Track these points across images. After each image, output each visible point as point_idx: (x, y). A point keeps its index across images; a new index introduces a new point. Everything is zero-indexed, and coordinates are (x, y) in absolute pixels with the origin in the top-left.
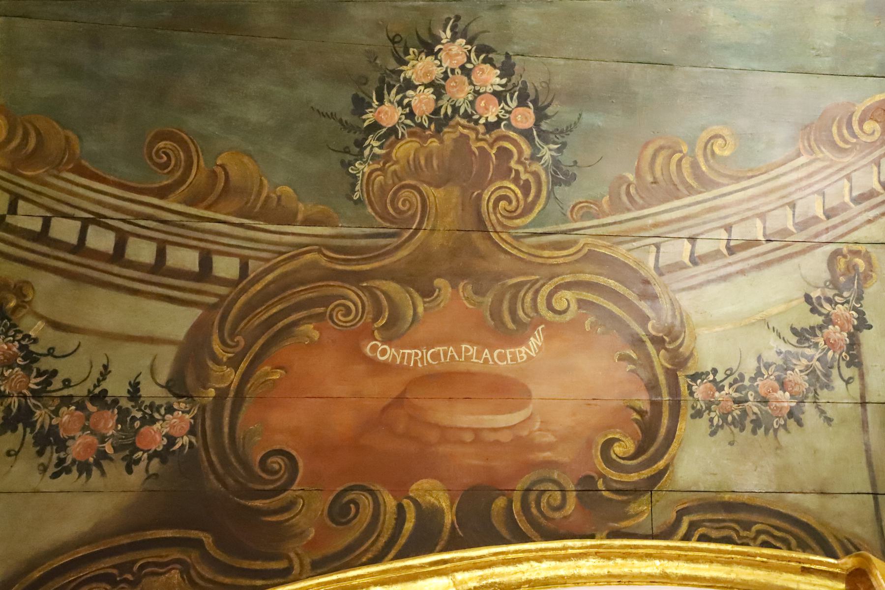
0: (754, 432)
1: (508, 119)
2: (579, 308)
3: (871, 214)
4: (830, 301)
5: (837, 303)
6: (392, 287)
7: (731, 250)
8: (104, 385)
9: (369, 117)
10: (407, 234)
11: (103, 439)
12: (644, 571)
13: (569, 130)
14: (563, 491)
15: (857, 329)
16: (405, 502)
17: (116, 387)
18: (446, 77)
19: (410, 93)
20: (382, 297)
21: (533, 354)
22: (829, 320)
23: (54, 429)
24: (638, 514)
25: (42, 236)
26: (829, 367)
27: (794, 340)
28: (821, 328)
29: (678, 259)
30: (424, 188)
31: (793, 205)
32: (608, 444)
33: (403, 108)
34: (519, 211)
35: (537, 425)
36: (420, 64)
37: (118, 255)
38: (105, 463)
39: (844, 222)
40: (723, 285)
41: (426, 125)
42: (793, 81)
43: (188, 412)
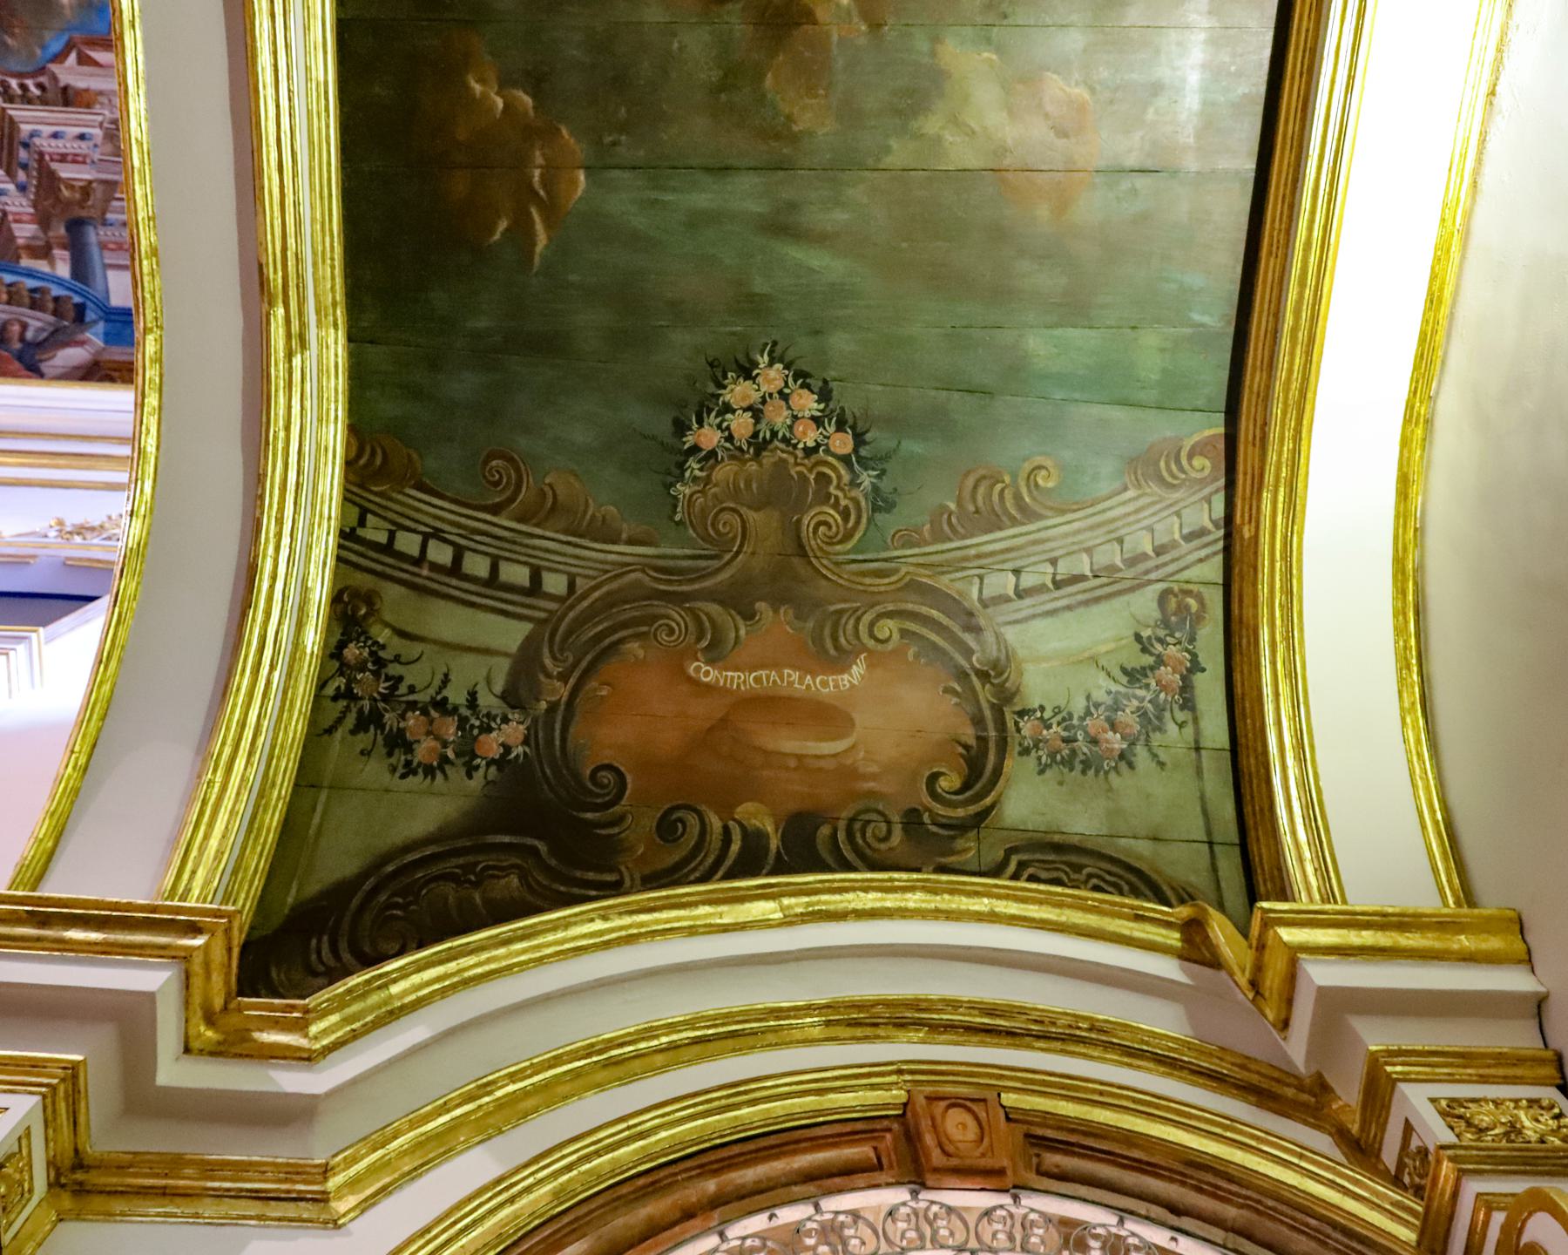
0: (1084, 772)
1: (827, 445)
2: (902, 637)
3: (1203, 553)
4: (1161, 641)
5: (1168, 644)
6: (714, 609)
7: (1058, 585)
9: (690, 440)
10: (727, 557)
13: (887, 457)
15: (1190, 671)
18: (764, 402)
19: (729, 416)
20: (704, 618)
21: (856, 682)
22: (1160, 661)
25: (388, 548)
26: (1160, 710)
27: (1124, 680)
28: (1152, 668)
29: (1002, 592)
30: (743, 510)
31: (1120, 541)
33: (722, 431)
34: (839, 537)
36: (738, 388)
37: (455, 569)
39: (1173, 561)
40: (1049, 621)
41: (745, 448)
42: (1116, 413)
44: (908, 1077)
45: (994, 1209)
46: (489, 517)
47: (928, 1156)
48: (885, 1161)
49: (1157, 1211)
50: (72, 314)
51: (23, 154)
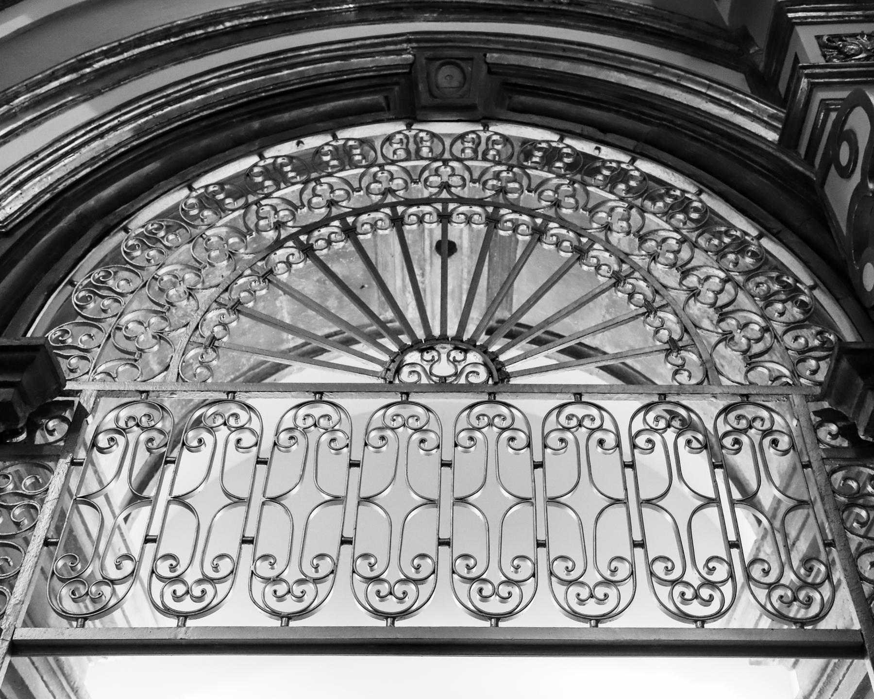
44: (414, 45)
45: (467, 133)
48: (392, 106)
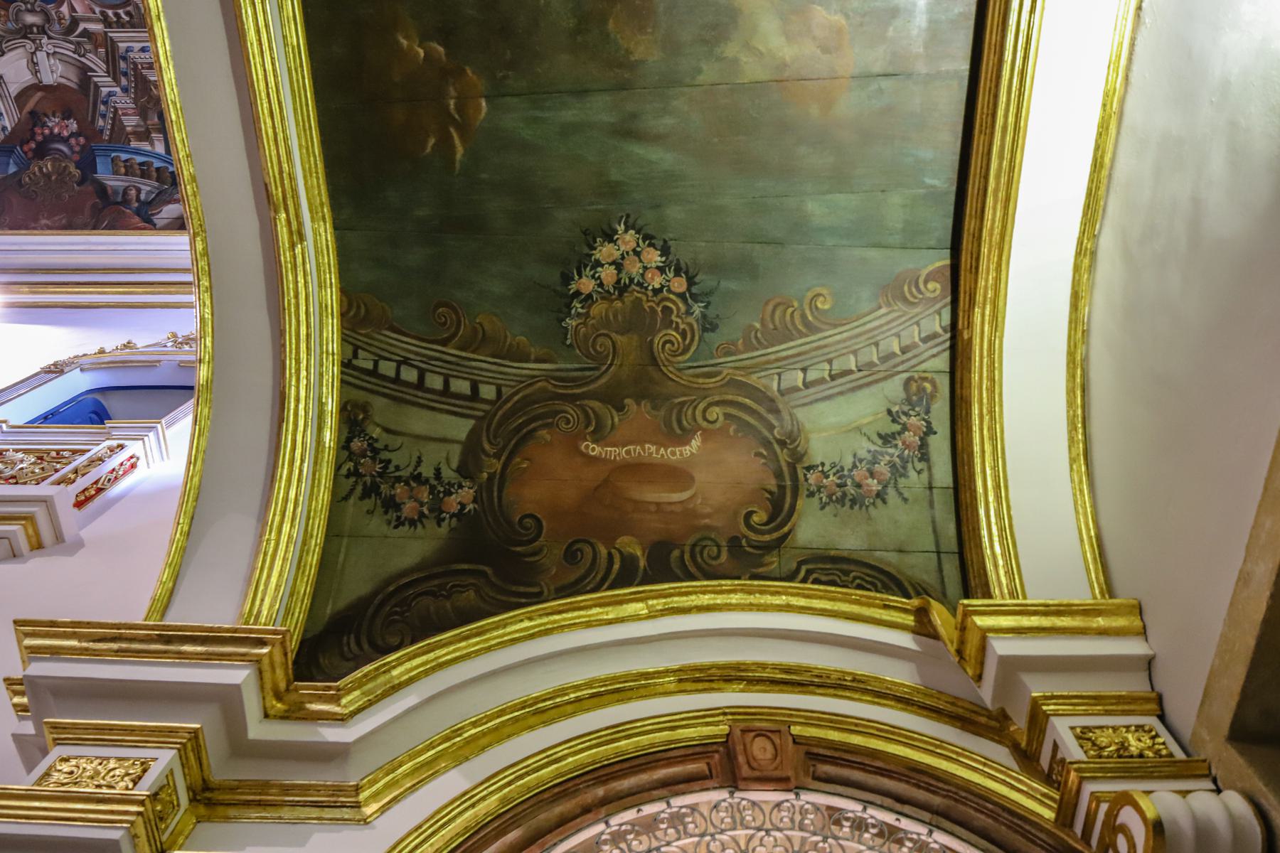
0: (852, 507)
1: (668, 286)
2: (725, 419)
3: (935, 351)
4: (906, 414)
5: (911, 416)
6: (596, 404)
7: (833, 378)
8: (419, 470)
9: (573, 287)
10: (604, 368)
11: (422, 504)
12: (774, 602)
13: (710, 293)
14: (718, 546)
15: (926, 434)
16: (613, 551)
17: (427, 471)
18: (623, 258)
19: (599, 269)
20: (590, 411)
21: (694, 451)
22: (905, 428)
23: (393, 497)
24: (772, 563)
25: (374, 373)
26: (905, 461)
27: (880, 442)
28: (899, 433)
29: (794, 384)
30: (613, 335)
31: (877, 344)
32: (749, 515)
33: (596, 280)
34: (680, 351)
35: (699, 501)
36: (605, 249)
37: (420, 385)
38: (424, 520)
39: (915, 356)
40: (827, 403)
41: (612, 291)
43: (472, 488)
44: (730, 717)
45: (782, 802)
46: (440, 348)
47: (739, 768)
48: (714, 771)
49: (888, 802)
50: (169, 180)
51: (123, 65)
